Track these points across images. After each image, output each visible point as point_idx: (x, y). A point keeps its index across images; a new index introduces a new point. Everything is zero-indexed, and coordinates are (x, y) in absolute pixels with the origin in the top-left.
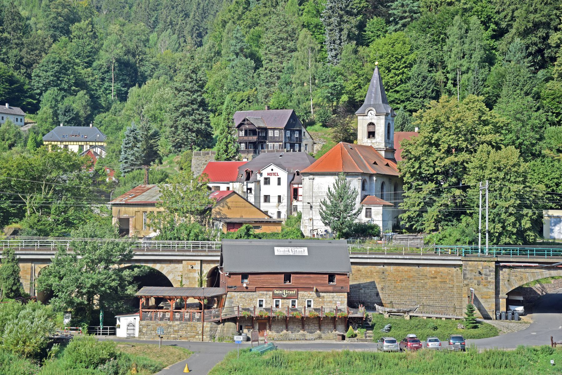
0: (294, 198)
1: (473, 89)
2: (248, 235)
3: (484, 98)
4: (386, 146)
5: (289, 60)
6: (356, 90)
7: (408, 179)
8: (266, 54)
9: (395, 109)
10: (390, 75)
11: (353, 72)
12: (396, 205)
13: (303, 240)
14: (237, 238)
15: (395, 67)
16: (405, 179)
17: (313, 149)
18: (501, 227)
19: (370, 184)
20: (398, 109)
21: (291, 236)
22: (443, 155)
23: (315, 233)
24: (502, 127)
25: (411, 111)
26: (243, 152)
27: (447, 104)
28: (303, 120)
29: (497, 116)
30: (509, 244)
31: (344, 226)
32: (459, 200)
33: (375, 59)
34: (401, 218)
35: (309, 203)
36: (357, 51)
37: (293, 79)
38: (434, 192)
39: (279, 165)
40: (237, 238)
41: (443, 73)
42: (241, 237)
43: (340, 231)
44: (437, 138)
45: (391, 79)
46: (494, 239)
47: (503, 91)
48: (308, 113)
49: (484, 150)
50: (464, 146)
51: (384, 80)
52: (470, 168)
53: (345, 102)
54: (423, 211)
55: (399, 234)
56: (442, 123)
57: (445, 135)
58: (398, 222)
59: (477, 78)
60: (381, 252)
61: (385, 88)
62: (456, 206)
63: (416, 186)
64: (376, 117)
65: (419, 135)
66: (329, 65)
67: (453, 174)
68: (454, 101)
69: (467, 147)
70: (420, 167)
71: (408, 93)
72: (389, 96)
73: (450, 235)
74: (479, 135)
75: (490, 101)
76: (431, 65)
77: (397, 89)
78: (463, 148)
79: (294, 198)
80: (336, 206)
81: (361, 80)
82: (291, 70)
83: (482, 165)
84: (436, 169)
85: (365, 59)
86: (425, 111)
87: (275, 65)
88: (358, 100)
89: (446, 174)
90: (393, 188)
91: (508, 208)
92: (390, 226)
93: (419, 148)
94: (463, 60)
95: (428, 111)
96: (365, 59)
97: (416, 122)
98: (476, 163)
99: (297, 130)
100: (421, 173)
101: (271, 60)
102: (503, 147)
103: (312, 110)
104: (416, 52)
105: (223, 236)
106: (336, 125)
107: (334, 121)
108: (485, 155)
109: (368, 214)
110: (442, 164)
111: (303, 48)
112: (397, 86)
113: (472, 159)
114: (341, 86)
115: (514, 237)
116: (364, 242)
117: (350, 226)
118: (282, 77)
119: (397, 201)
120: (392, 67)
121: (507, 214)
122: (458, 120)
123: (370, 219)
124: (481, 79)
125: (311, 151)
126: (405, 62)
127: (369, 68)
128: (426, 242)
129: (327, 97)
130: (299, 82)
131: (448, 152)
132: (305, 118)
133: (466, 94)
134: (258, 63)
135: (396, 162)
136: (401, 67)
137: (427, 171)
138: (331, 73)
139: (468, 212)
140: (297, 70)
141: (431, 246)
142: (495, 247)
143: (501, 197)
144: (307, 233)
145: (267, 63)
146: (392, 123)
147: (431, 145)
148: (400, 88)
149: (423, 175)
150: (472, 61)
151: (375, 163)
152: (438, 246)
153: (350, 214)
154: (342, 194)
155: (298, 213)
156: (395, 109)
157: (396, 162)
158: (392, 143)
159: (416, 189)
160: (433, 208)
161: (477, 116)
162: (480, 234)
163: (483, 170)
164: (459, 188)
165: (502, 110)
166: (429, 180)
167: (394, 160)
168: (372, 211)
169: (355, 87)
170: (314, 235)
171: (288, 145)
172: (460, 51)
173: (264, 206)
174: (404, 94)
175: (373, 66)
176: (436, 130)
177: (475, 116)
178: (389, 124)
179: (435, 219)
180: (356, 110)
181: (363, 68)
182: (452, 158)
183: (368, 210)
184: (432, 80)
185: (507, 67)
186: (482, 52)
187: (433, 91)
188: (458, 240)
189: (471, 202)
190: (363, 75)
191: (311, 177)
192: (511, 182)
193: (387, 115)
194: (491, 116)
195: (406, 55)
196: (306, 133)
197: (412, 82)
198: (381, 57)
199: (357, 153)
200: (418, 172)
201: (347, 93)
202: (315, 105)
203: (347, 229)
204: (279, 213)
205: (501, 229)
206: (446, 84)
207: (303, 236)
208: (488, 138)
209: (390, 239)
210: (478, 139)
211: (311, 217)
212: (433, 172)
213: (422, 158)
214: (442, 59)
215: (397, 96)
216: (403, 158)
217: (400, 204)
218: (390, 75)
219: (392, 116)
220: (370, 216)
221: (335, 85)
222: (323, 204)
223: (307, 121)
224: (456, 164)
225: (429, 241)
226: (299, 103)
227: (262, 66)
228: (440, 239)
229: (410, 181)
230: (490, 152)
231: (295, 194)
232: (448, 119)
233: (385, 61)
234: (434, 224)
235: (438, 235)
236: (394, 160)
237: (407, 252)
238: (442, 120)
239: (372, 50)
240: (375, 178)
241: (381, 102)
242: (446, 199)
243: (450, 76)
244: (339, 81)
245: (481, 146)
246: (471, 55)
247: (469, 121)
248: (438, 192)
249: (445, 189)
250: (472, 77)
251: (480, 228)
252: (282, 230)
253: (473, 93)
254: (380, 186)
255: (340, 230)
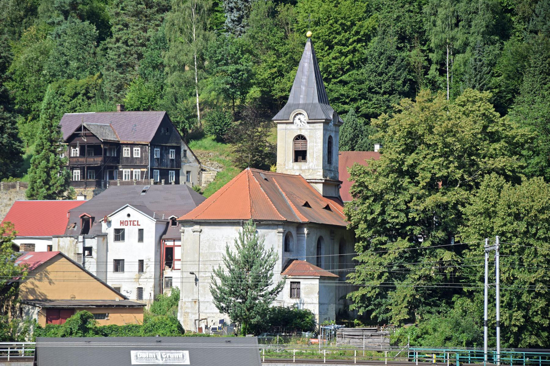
0: (167, 264)
1: (473, 80)
2: (84, 329)
3: (491, 95)
4: (324, 176)
5: (158, 25)
6: (273, 79)
7: (363, 232)
8: (118, 14)
9: (341, 113)
10: (333, 55)
11: (269, 48)
12: (342, 276)
13: (182, 338)
14: (64, 336)
15: (340, 41)
16: (358, 232)
17: (200, 180)
18: (523, 317)
19: (298, 240)
20: (346, 112)
21: (161, 331)
22: (423, 191)
23: (203, 325)
24: (523, 145)
25: (368, 117)
26: (77, 184)
27: (429, 104)
28: (183, 130)
29: (514, 125)
30: (537, 346)
31: (253, 314)
32: (450, 269)
33: (307, 27)
34: (351, 299)
35: (192, 273)
36: (277, 12)
37: (166, 59)
38: (407, 255)
39: (141, 208)
40: (64, 336)
41: (423, 51)
42: (71, 333)
43: (246, 322)
44: (411, 162)
45: (333, 61)
46: (509, 338)
47: (525, 83)
48: (191, 117)
49: (492, 184)
50: (458, 176)
51: (321, 63)
52: (468, 214)
53: (255, 99)
54: (386, 288)
55: (346, 327)
56: (420, 138)
57: (425, 158)
58: (346, 306)
59: (480, 60)
60: (316, 358)
61: (323, 77)
62: (445, 279)
63: (376, 245)
64: (308, 126)
65: (381, 157)
66: (228, 35)
67: (440, 224)
68: (440, 100)
69: (462, 178)
70: (383, 212)
71: (363, 86)
72: (331, 90)
73: (435, 330)
74: (484, 158)
75: (503, 101)
76: (402, 38)
77: (344, 78)
78: (456, 181)
79: (167, 264)
80: (240, 278)
81: (282, 63)
82: (162, 43)
83: (488, 209)
84: (411, 216)
85: (290, 27)
86: (391, 117)
87: (134, 33)
88: (277, 97)
89: (427, 223)
90: (337, 247)
91: (534, 284)
92: (332, 314)
93: (381, 179)
94: (456, 30)
95: (397, 116)
96: (290, 27)
97: (377, 134)
98: (478, 205)
99: (173, 147)
100: (384, 222)
101: (126, 26)
102: (524, 178)
103: (198, 113)
104: (376, 14)
105: (40, 332)
106: (240, 140)
107: (236, 132)
108: (493, 192)
109: (295, 291)
110: (421, 207)
111: (182, 6)
112: (344, 73)
113: (472, 198)
114: (248, 71)
115: (545, 334)
116: (287, 341)
117: (263, 313)
118: (146, 55)
119: (344, 270)
120: (336, 41)
121: (532, 294)
122: (448, 131)
123: (298, 301)
124: (486, 62)
125: (196, 184)
126: (357, 33)
127: (297, 42)
128: (393, 341)
129: (225, 91)
130: (176, 64)
131: (431, 187)
132: (187, 125)
133: (461, 87)
134: (104, 30)
135: (341, 203)
136: (351, 40)
137: (395, 218)
138: (232, 49)
139: (465, 289)
140: (172, 43)
141: (402, 348)
142: (513, 351)
143: (521, 265)
144: (188, 326)
145: (120, 30)
146: (336, 136)
147: (401, 173)
148: (350, 76)
149: (388, 226)
150: (471, 32)
151: (307, 205)
152: (414, 349)
153: (263, 293)
154: (250, 259)
155: (173, 290)
156: (341, 113)
157: (341, 203)
158: (336, 171)
159: (376, 250)
160: (405, 282)
161: (478, 127)
162: (486, 328)
163: (490, 218)
164: (449, 249)
165: (522, 117)
166: (400, 235)
167: (339, 200)
168: (302, 286)
169: (272, 74)
170: (200, 329)
171: (157, 173)
172: (450, 14)
173: (113, 279)
174: (357, 87)
175: (303, 38)
176: (409, 149)
177: (477, 126)
178: (330, 138)
179: (409, 302)
180: (275, 113)
181: (287, 42)
182: (439, 197)
183: (294, 286)
184: (405, 63)
185: (531, 41)
186: (489, 15)
187: (404, 83)
188: (448, 339)
189: (470, 272)
190: (286, 54)
191: (197, 227)
192: (539, 239)
193: (327, 122)
194: (504, 125)
195: (360, 20)
196: (188, 152)
197: (370, 66)
198: (317, 23)
199: (276, 187)
200: (379, 220)
201: (258, 84)
202: (205, 104)
203: (258, 318)
204: (140, 291)
205: (522, 320)
206: (427, 69)
207: (181, 330)
208: (500, 162)
209: (332, 336)
210: (481, 165)
211: (196, 297)
212: (405, 220)
213: (386, 197)
214: (420, 28)
215: (343, 90)
216: (355, 196)
217: (349, 275)
218: (333, 55)
219: (335, 125)
220: (298, 296)
221: (238, 71)
222: (218, 275)
223: (190, 131)
224: (444, 207)
225: (399, 341)
226: (176, 99)
227: (111, 36)
228: (418, 337)
229: (366, 235)
230: (502, 187)
231: (168, 258)
232: (430, 130)
233: (322, 30)
234: (406, 310)
235: (413, 330)
236: (339, 200)
237: (361, 359)
238: (420, 132)
239: (302, 11)
240: (306, 231)
241: (316, 100)
242: (427, 267)
243: (433, 56)
244: (244, 64)
245: (486, 176)
246: (469, 22)
247: (467, 134)
248: (414, 255)
249: (425, 249)
250: (472, 60)
251: (486, 318)
252: (145, 321)
253: (474, 87)
254: (314, 244)
255: (246, 321)
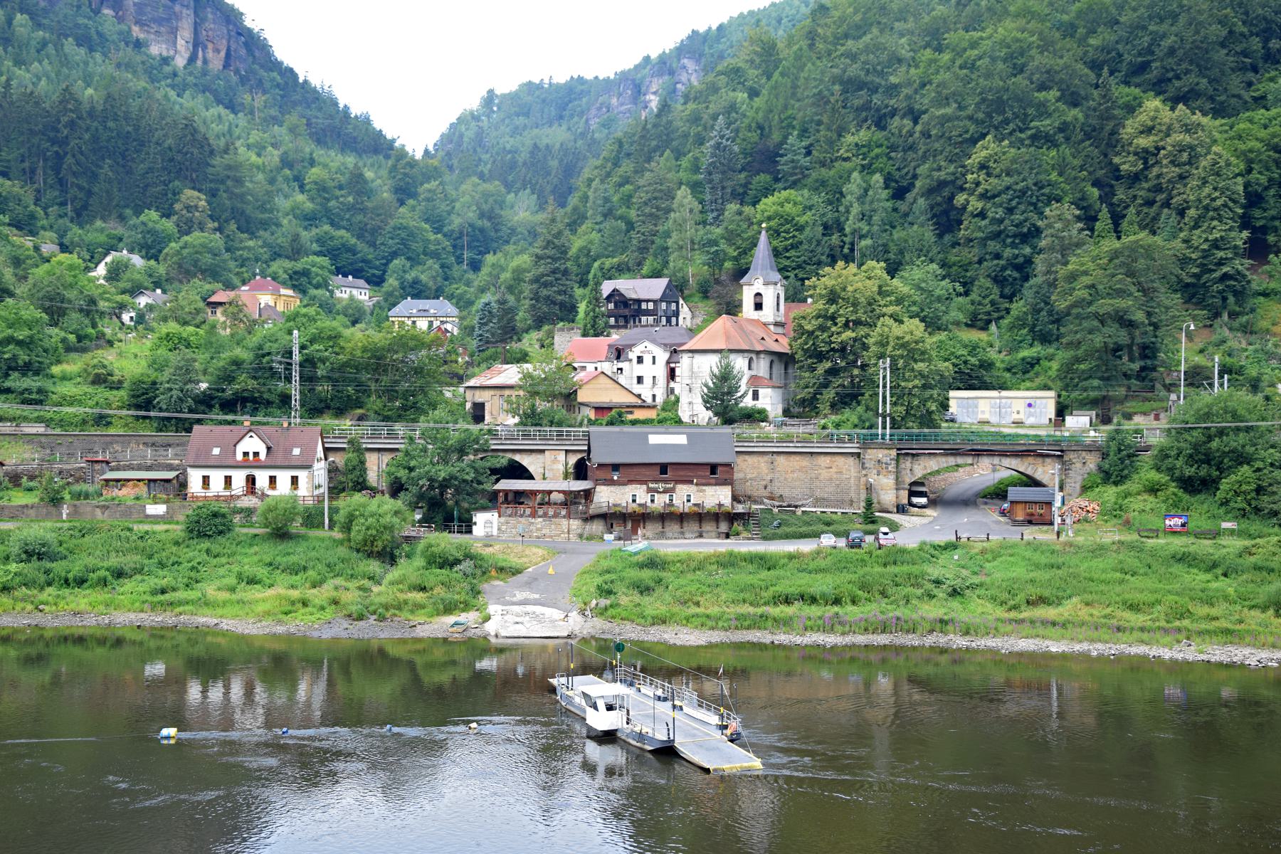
26: (612, 327)
39: (653, 341)
105: (591, 423)
109: (756, 396)
144: (685, 419)
204: (654, 396)
231: (672, 374)
246: (871, 217)
